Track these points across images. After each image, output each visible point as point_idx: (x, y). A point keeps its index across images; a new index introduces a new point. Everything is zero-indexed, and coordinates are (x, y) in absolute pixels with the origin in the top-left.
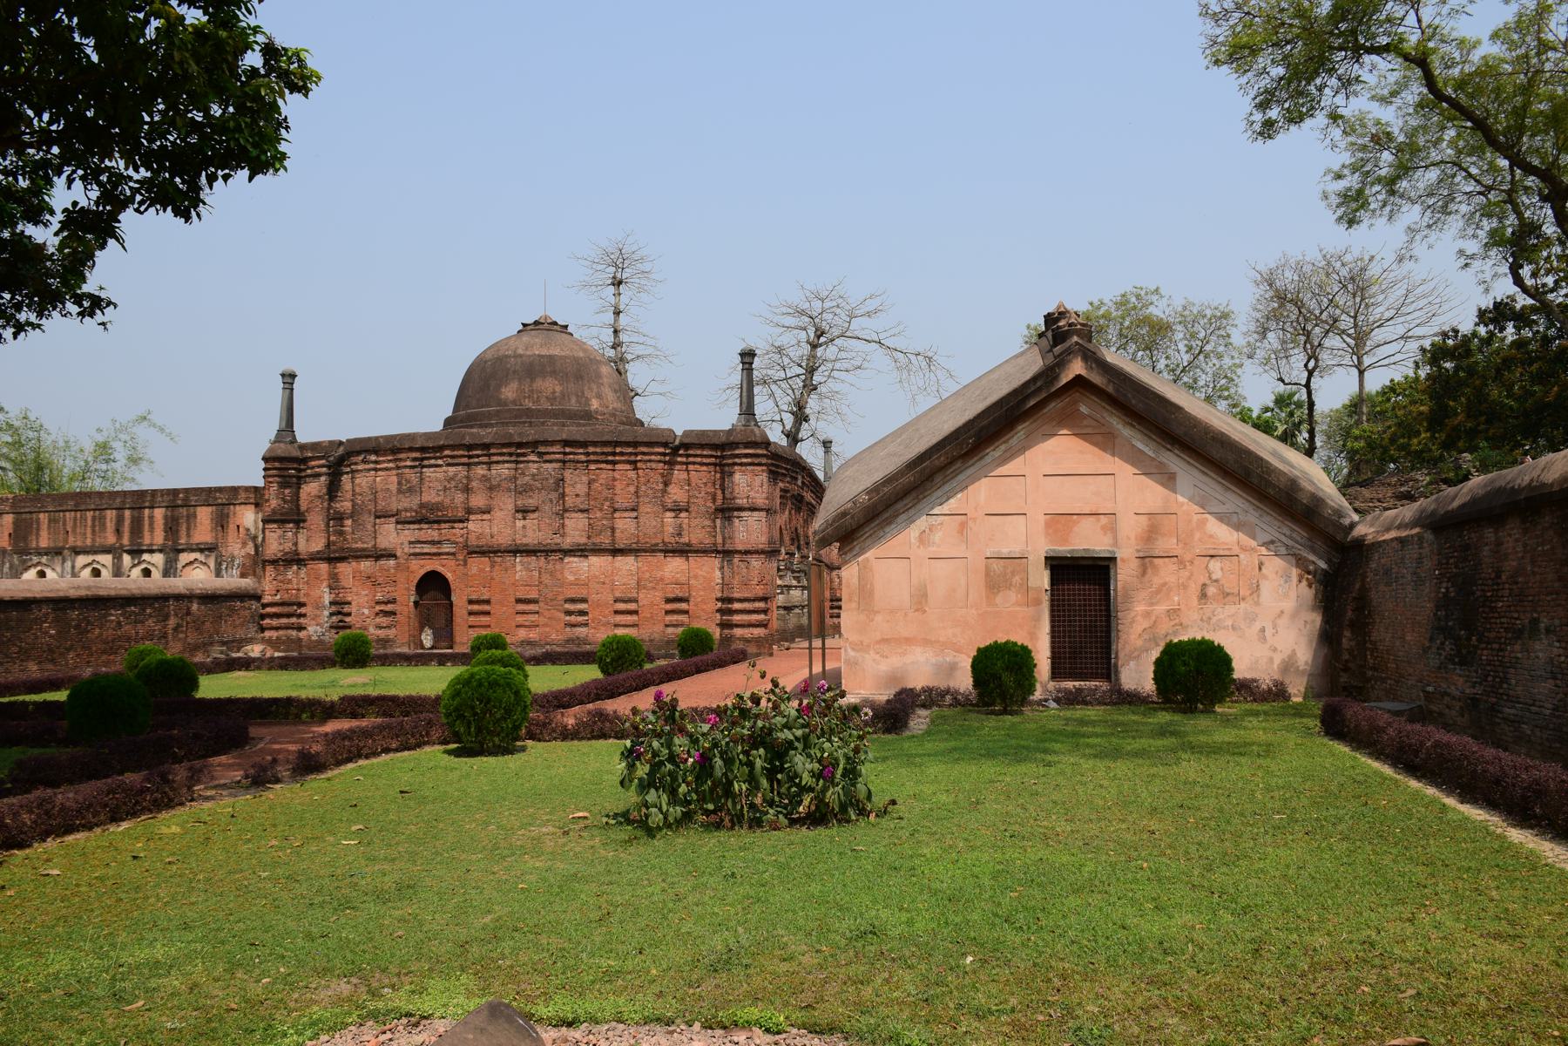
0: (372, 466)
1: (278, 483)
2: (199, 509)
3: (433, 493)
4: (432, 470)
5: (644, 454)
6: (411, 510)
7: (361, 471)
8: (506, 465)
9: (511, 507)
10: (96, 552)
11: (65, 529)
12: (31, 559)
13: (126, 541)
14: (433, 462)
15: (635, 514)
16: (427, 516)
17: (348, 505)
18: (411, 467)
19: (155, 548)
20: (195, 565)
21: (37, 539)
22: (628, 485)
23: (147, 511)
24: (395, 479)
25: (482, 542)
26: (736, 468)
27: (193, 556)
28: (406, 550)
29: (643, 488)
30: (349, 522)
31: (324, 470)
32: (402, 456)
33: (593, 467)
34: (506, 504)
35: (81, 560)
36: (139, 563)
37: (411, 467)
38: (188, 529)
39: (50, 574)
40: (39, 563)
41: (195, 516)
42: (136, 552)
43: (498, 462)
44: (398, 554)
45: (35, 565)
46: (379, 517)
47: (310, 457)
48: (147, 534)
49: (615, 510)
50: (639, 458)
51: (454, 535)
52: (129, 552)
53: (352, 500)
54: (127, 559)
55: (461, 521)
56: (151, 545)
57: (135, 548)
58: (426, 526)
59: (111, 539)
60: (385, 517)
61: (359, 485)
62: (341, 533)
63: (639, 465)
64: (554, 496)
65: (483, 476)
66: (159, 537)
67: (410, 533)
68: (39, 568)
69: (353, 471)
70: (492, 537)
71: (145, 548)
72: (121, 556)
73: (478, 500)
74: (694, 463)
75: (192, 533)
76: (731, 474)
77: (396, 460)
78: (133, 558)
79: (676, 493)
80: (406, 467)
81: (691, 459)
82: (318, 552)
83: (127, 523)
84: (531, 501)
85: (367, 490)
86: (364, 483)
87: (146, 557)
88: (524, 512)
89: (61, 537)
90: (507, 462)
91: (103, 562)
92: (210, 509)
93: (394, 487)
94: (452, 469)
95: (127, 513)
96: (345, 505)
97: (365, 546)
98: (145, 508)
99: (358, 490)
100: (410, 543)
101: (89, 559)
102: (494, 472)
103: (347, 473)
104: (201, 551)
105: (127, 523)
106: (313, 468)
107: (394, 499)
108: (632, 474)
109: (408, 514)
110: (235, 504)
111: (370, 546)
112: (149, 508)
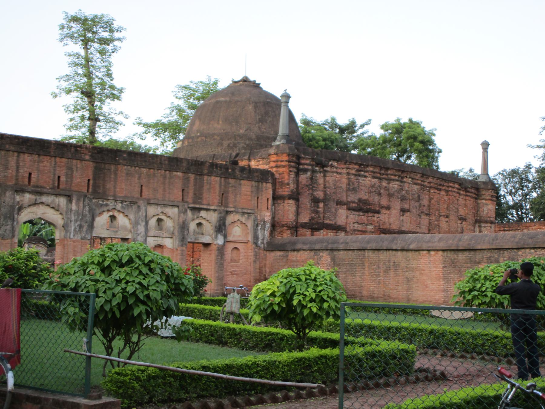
0: (335, 170)
1: (295, 172)
2: (243, 182)
3: (363, 193)
4: (362, 178)
5: (452, 187)
6: (354, 202)
8: (397, 183)
9: (398, 208)
14: (363, 173)
15: (447, 219)
18: (355, 175)
19: (212, 208)
20: (236, 224)
21: (115, 188)
22: (444, 203)
24: (345, 181)
25: (385, 227)
27: (237, 217)
29: (451, 206)
30: (321, 205)
31: (310, 167)
32: (351, 166)
33: (432, 191)
34: (397, 206)
35: (152, 210)
36: (197, 218)
37: (355, 175)
39: (122, 220)
43: (394, 180)
44: (348, 230)
45: (108, 210)
46: (337, 204)
47: (303, 158)
49: (440, 216)
50: (450, 189)
51: (374, 221)
52: (193, 209)
54: (189, 213)
55: (378, 212)
57: (197, 206)
58: (361, 214)
59: (177, 194)
61: (328, 181)
62: (317, 212)
63: (450, 193)
64: (417, 204)
65: (386, 187)
67: (354, 216)
69: (326, 171)
70: (390, 225)
71: (205, 207)
72: (186, 211)
73: (384, 202)
74: (469, 196)
77: (347, 168)
78: (193, 214)
79: (462, 212)
81: (468, 194)
82: (305, 223)
84: (406, 206)
85: (332, 186)
86: (330, 181)
87: (203, 213)
88: (403, 211)
89: (138, 189)
90: (398, 181)
91: (170, 214)
93: (344, 186)
94: (373, 180)
95: (192, 176)
96: (320, 194)
97: (331, 222)
99: (327, 185)
100: (354, 223)
101: (159, 209)
102: (391, 186)
106: (304, 164)
107: (344, 193)
108: (446, 198)
109: (354, 205)
110: (266, 183)
111: (333, 223)
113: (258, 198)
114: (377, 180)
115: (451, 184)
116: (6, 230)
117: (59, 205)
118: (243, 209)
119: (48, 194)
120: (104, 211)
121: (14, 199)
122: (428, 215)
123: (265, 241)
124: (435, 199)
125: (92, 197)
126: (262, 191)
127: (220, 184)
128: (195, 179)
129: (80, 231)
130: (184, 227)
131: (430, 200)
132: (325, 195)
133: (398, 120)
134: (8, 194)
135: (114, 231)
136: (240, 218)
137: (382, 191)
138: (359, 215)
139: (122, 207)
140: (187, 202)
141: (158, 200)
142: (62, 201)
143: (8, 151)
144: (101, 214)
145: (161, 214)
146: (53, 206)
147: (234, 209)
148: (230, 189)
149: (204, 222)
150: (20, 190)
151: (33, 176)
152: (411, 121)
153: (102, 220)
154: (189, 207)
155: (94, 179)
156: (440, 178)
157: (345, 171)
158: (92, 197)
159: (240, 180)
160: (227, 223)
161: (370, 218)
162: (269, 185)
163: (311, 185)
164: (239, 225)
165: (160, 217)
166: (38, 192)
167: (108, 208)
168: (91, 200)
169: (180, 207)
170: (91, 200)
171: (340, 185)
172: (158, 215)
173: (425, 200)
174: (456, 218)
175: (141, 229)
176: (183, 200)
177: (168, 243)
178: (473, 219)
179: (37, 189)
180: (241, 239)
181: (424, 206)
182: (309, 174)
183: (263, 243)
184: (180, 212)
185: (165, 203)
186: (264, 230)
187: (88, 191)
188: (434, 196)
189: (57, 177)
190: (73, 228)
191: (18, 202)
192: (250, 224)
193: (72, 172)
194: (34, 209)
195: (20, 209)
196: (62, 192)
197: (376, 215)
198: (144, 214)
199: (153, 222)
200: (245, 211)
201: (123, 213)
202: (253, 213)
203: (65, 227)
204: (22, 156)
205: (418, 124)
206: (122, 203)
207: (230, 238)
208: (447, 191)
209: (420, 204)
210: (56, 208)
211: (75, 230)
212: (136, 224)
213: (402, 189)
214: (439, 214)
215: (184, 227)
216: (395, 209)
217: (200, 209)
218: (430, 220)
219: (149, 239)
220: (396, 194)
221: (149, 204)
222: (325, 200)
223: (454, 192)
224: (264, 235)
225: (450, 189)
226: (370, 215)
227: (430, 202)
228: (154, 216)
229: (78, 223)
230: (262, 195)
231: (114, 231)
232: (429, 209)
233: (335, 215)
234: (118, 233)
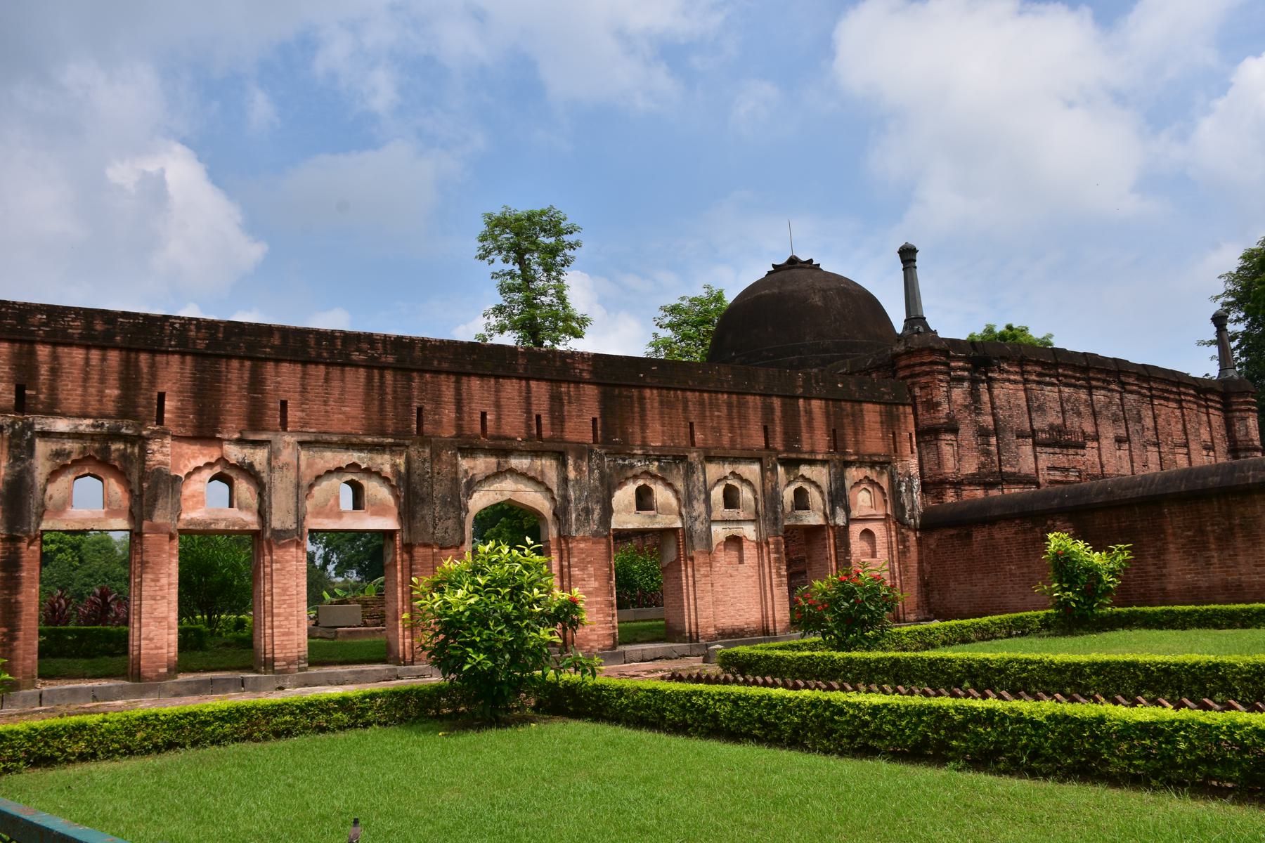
4: (1049, 388)
6: (1043, 431)
7: (998, 380)
9: (1111, 435)
10: (736, 460)
11: (687, 419)
12: (632, 466)
13: (778, 444)
14: (1048, 379)
16: (1060, 440)
17: (990, 419)
19: (820, 457)
21: (643, 430)
22: (1177, 422)
23: (801, 401)
24: (1022, 394)
26: (1250, 413)
28: (1046, 477)
30: (993, 440)
31: (966, 373)
32: (1029, 368)
33: (1156, 402)
35: (714, 471)
37: (1039, 383)
38: (856, 434)
39: (662, 494)
40: (647, 473)
41: (862, 416)
42: (792, 464)
44: (1041, 480)
45: (636, 477)
46: (1018, 437)
48: (805, 435)
51: (1079, 462)
53: (994, 415)
54: (780, 469)
56: (812, 452)
57: (793, 456)
58: (1057, 450)
60: (1023, 437)
62: (987, 453)
64: (1138, 427)
66: (818, 440)
67: (1047, 458)
68: (641, 482)
71: (806, 456)
74: (1212, 407)
75: (860, 438)
76: (1245, 419)
78: (788, 472)
80: (1034, 381)
82: (973, 475)
83: (778, 413)
85: (1005, 404)
86: (1001, 397)
87: (805, 470)
89: (684, 431)
90: (1103, 388)
91: (746, 475)
92: (877, 407)
96: (987, 420)
97: (1013, 470)
98: (798, 397)
99: (998, 403)
100: (1049, 468)
101: (727, 469)
103: (983, 382)
104: (872, 465)
105: (778, 413)
111: (1017, 470)
112: (805, 398)
113: (894, 434)
114: (1072, 390)
115: (1182, 389)
116: (447, 528)
117: (542, 473)
118: (870, 455)
119: (521, 453)
120: (627, 479)
121: (456, 465)
122: (1157, 445)
123: (916, 513)
124: (1163, 417)
125: (603, 451)
126: (899, 420)
127: (827, 414)
128: (783, 405)
129: (587, 520)
130: (771, 498)
131: (1155, 418)
132: (996, 421)
133: (990, 330)
134: (446, 455)
135: (650, 516)
136: (867, 472)
137: (1082, 408)
138: (1054, 454)
139: (660, 468)
140: (775, 449)
141: (724, 448)
142: (548, 467)
143: (438, 372)
144: (621, 485)
145: (731, 477)
146: (532, 474)
147: (856, 457)
148: (845, 421)
149: (806, 486)
150: (470, 450)
151: (488, 417)
152: (1010, 327)
153: (625, 496)
154: (779, 459)
155: (603, 415)
156: (1165, 380)
157: (1018, 378)
158: (603, 451)
159: (860, 402)
160: (848, 484)
161: (1070, 457)
162: (909, 410)
163: (971, 405)
164: (865, 486)
165: (729, 482)
166: (502, 449)
167: (634, 472)
168: (601, 458)
169: (764, 461)
170: (601, 458)
171: (1017, 402)
172: (726, 478)
173: (1147, 420)
174: (1199, 447)
175: (699, 508)
176: (767, 446)
177: (749, 531)
178: (1224, 446)
179: (498, 442)
180: (873, 512)
181: (1148, 429)
182: (966, 384)
183: (912, 517)
184: (763, 470)
185: (737, 453)
186: (912, 492)
187: (595, 442)
188: (1160, 410)
189: (534, 418)
190: (574, 516)
191: (466, 472)
192: (884, 481)
193: (562, 404)
194: (496, 486)
195: (473, 485)
196: (547, 446)
197: (1081, 452)
198: (702, 479)
199: (717, 493)
200: (877, 459)
201: (663, 480)
202: (889, 463)
203: (561, 514)
204: (465, 380)
205: (1023, 331)
206: (659, 460)
207: (855, 513)
208: (1180, 402)
209: (1143, 426)
210: (537, 481)
211: (577, 519)
212: (686, 500)
213: (1110, 402)
214: (1172, 442)
215: (771, 498)
216: (1106, 438)
217: (797, 463)
218: (1160, 452)
219: (714, 528)
220: (1104, 412)
221: (709, 459)
222: (997, 431)
223: (1190, 401)
224: (913, 502)
225: (1183, 397)
226: (1071, 451)
227: (1155, 422)
228: (719, 481)
229: (583, 504)
230: (899, 428)
231: (650, 516)
232: (1157, 434)
233: (1017, 456)
234: (657, 520)
